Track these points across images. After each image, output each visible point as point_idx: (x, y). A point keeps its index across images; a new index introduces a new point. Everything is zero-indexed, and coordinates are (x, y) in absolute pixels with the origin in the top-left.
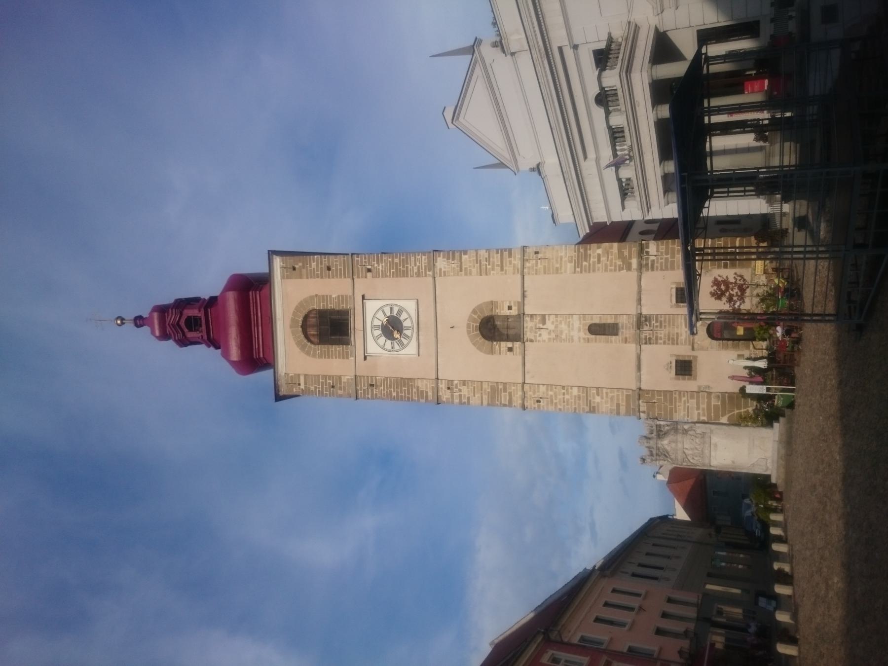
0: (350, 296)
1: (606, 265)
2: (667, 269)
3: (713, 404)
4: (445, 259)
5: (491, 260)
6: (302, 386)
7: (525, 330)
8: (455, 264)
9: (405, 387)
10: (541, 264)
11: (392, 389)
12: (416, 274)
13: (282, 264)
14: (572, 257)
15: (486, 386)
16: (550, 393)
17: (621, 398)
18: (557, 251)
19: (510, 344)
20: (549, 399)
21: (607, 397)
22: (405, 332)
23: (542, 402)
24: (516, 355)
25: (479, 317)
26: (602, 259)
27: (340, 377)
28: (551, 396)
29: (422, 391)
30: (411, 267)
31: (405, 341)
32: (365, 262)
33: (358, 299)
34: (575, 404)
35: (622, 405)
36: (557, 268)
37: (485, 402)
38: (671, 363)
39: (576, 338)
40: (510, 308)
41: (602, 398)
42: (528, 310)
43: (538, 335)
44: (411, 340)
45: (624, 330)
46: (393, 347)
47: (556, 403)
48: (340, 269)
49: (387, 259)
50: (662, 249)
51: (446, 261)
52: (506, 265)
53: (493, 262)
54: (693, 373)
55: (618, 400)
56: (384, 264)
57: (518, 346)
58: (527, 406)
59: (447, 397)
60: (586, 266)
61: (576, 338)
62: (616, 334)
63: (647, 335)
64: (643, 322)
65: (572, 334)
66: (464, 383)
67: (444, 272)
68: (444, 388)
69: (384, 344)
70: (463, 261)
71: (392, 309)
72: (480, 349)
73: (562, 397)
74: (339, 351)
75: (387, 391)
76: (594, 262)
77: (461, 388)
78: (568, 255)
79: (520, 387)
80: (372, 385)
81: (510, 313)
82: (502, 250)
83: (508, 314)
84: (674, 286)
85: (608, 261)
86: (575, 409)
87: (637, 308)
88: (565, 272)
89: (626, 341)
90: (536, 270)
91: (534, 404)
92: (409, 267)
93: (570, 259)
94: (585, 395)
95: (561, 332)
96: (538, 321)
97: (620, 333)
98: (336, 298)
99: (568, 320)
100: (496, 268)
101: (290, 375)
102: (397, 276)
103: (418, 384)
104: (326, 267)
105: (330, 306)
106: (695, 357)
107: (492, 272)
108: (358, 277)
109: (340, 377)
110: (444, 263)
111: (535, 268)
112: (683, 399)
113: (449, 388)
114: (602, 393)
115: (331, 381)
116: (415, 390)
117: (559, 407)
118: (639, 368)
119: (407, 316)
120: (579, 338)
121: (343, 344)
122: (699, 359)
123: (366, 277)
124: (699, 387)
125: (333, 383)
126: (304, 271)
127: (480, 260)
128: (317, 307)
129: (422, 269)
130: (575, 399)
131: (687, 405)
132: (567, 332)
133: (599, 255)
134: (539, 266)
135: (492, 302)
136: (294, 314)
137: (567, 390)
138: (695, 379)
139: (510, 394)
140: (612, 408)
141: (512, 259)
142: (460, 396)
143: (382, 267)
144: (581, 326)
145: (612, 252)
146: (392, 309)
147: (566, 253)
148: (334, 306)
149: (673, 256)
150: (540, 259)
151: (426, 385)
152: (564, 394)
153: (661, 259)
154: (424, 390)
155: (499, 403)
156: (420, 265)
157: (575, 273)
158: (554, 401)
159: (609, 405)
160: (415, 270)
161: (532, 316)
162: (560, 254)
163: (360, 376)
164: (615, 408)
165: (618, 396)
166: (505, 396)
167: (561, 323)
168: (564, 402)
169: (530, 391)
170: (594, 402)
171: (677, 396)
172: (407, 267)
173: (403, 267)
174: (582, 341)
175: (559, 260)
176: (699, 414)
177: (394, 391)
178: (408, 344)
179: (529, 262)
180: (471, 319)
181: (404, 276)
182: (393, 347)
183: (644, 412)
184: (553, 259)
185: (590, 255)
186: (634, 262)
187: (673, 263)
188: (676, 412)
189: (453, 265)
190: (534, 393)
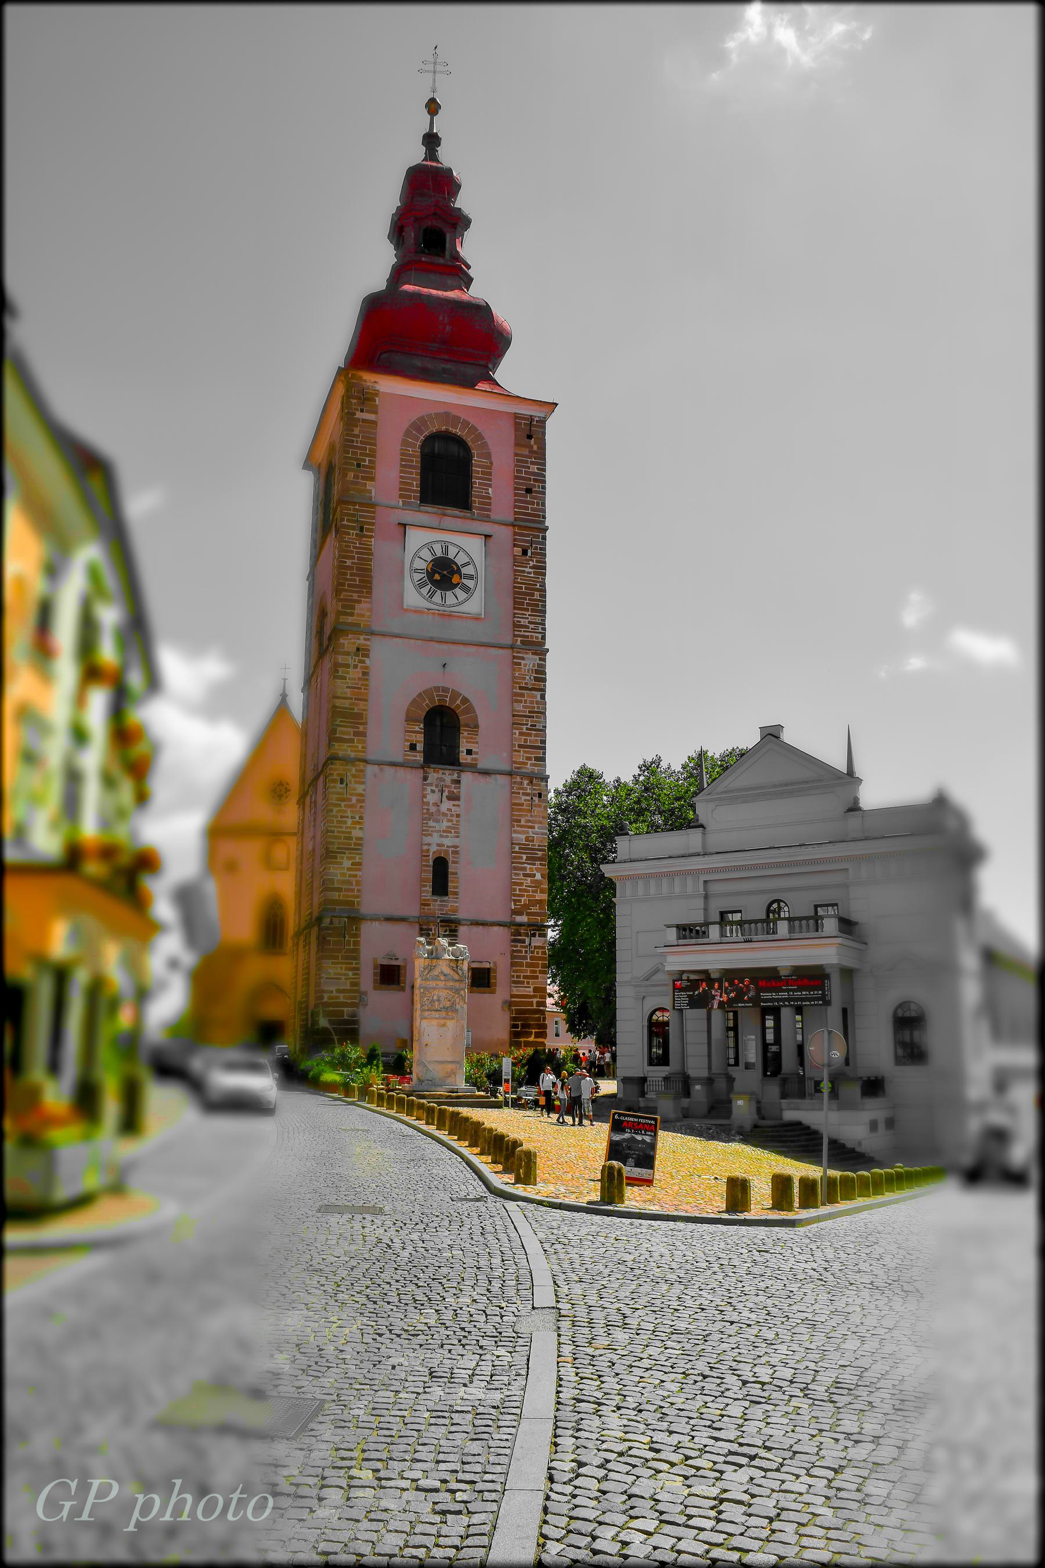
0: (488, 516)
1: (521, 884)
2: (513, 957)
3: (345, 1009)
4: (536, 668)
5: (533, 732)
6: (359, 415)
7: (441, 772)
8: (529, 680)
10: (525, 800)
12: (518, 621)
13: (536, 419)
15: (362, 707)
16: (354, 799)
17: (350, 893)
18: (540, 823)
19: (420, 747)
20: (345, 796)
22: (439, 592)
23: (342, 785)
24: (406, 755)
25: (458, 706)
26: (529, 879)
27: (372, 479)
28: (350, 800)
29: (353, 608)
30: (527, 616)
31: (425, 591)
32: (536, 548)
33: (487, 528)
34: (339, 832)
35: (339, 895)
36: (520, 821)
37: (338, 702)
38: (397, 959)
39: (426, 840)
40: (469, 752)
41: (349, 869)
42: (467, 778)
43: (434, 788)
46: (416, 570)
47: (340, 805)
48: (527, 508)
49: (539, 582)
50: (538, 953)
52: (525, 752)
53: (530, 735)
54: (384, 986)
55: (347, 890)
56: (532, 575)
57: (418, 758)
58: (335, 764)
59: (346, 645)
60: (521, 858)
61: (426, 840)
62: (434, 893)
63: (433, 932)
64: (448, 926)
65: (435, 835)
67: (520, 664)
68: (358, 642)
70: (533, 692)
71: (470, 577)
72: (414, 703)
73: (349, 814)
76: (525, 869)
77: (359, 669)
79: (361, 755)
80: (362, 529)
81: (463, 752)
82: (545, 748)
84: (492, 965)
86: (333, 832)
87: (467, 920)
88: (516, 832)
89: (424, 904)
90: (519, 793)
91: (338, 775)
92: (527, 613)
94: (353, 846)
95: (437, 821)
97: (435, 898)
99: (453, 831)
101: (377, 399)
102: (515, 593)
103: (366, 602)
105: (476, 482)
106: (403, 989)
107: (517, 732)
108: (515, 534)
110: (531, 665)
111: (521, 791)
112: (350, 973)
113: (358, 649)
114: (356, 870)
115: (367, 463)
116: (355, 596)
117: (335, 809)
118: (389, 919)
120: (429, 844)
121: (421, 492)
122: (401, 994)
123: (515, 545)
124: (365, 993)
125: (364, 466)
126: (526, 452)
127: (533, 717)
128: (475, 460)
129: (524, 631)
131: (343, 977)
132: (437, 828)
133: (534, 875)
134: (524, 798)
135: (477, 726)
136: (466, 424)
137: (359, 823)
138: (375, 988)
139: (351, 741)
141: (533, 762)
142: (347, 666)
143: (528, 573)
144: (445, 848)
145: (536, 892)
146: (470, 577)
148: (476, 488)
149: (528, 965)
150: (532, 798)
151: (363, 616)
153: (526, 952)
154: (356, 612)
155: (338, 723)
156: (530, 630)
157: (512, 844)
158: (343, 804)
159: (339, 877)
160: (523, 622)
161: (458, 782)
162: (536, 826)
164: (336, 885)
165: (353, 890)
168: (342, 817)
169: (356, 771)
170: (342, 858)
172: (527, 610)
174: (425, 847)
175: (531, 824)
176: (332, 992)
177: (353, 563)
178: (421, 594)
179: (528, 784)
180: (455, 695)
181: (515, 603)
183: (331, 923)
184: (531, 816)
185: (534, 864)
186: (523, 919)
187: (521, 965)
188: (333, 963)
189: (528, 677)
190: (354, 776)
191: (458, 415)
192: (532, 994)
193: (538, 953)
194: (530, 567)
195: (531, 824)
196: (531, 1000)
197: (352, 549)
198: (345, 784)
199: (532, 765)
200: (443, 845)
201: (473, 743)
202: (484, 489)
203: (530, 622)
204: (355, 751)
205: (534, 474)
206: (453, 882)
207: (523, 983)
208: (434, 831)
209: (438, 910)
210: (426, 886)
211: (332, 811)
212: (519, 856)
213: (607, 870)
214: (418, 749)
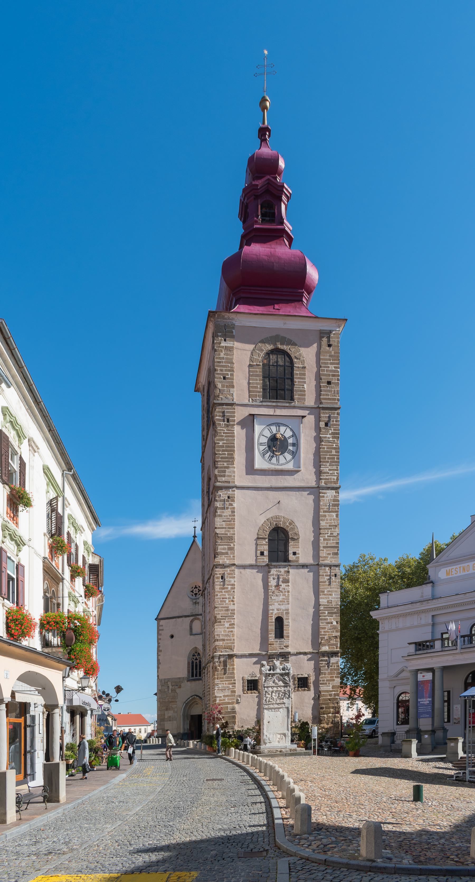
1: (325, 628)
5: (332, 538)
9: (228, 454)
11: (225, 442)
14: (331, 603)
15: (232, 532)
18: (336, 592)
19: (266, 553)
21: (229, 632)
26: (329, 625)
29: (225, 472)
35: (223, 643)
36: (324, 592)
40: (294, 553)
41: (228, 628)
44: (268, 462)
45: (278, 643)
46: (261, 444)
51: (332, 499)
53: (330, 540)
54: (249, 692)
56: (331, 439)
57: (265, 560)
59: (221, 495)
60: (325, 613)
62: (276, 637)
66: (233, 512)
67: (324, 497)
69: (264, 436)
70: (331, 513)
73: (227, 596)
74: (257, 387)
75: (223, 436)
76: (327, 619)
77: (229, 510)
78: (333, 600)
82: (338, 547)
83: (290, 552)
85: (328, 629)
90: (323, 575)
91: (220, 574)
93: (330, 601)
94: (229, 615)
96: (285, 577)
97: (276, 640)
98: (304, 388)
99: (286, 601)
100: (326, 542)
104: (330, 381)
109: (233, 387)
110: (330, 497)
111: (325, 574)
112: (231, 686)
113: (229, 497)
119: (288, 459)
120: (273, 610)
125: (228, 378)
127: (331, 529)
129: (326, 476)
130: (226, 607)
139: (227, 553)
140: (221, 636)
141: (331, 556)
143: (328, 438)
145: (333, 632)
147: (334, 598)
148: (297, 385)
152: (229, 598)
154: (226, 474)
158: (223, 591)
159: (223, 633)
161: (288, 572)
163: (234, 409)
165: (230, 640)
166: (224, 549)
167: (285, 595)
168: (223, 598)
169: (230, 571)
171: (233, 682)
172: (328, 462)
173: (328, 458)
175: (330, 593)
176: (221, 697)
177: (223, 443)
179: (329, 570)
182: (261, 444)
185: (332, 616)
188: (221, 681)
190: (228, 574)
191: (285, 336)
192: (331, 689)
193: (334, 666)
194: (330, 434)
195: (330, 593)
196: (331, 693)
197: (222, 434)
198: (224, 579)
199: (331, 558)
200: (281, 610)
201: (297, 548)
202: (301, 385)
203: (329, 470)
204: (229, 559)
205: (331, 371)
206: (286, 630)
207: (326, 684)
208: (275, 602)
209: (278, 647)
210: (271, 634)
211: (217, 595)
212: (324, 612)
213: (374, 614)
214: (265, 554)
